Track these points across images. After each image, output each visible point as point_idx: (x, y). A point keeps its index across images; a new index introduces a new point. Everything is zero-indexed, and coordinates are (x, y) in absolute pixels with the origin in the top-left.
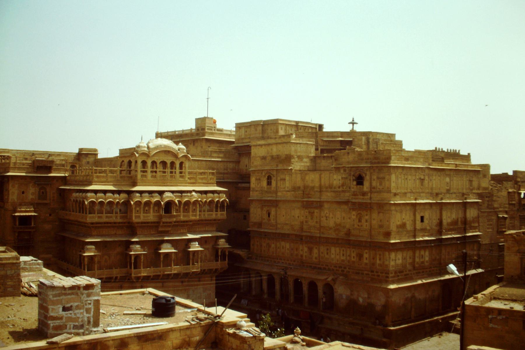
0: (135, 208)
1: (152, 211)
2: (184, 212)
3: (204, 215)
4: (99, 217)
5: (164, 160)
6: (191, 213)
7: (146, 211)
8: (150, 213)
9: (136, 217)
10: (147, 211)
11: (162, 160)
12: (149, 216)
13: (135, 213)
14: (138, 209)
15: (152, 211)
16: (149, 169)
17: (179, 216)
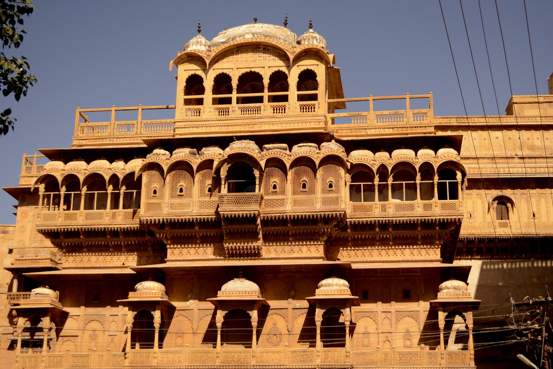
0: (149, 184)
1: (196, 189)
2: (294, 193)
3: (384, 209)
4: (68, 217)
5: (253, 70)
6: (319, 194)
7: (179, 193)
8: (191, 197)
9: (150, 206)
10: (181, 190)
11: (248, 70)
12: (188, 205)
13: (148, 197)
14: (156, 185)
15: (196, 189)
16: (208, 96)
17: (282, 202)
